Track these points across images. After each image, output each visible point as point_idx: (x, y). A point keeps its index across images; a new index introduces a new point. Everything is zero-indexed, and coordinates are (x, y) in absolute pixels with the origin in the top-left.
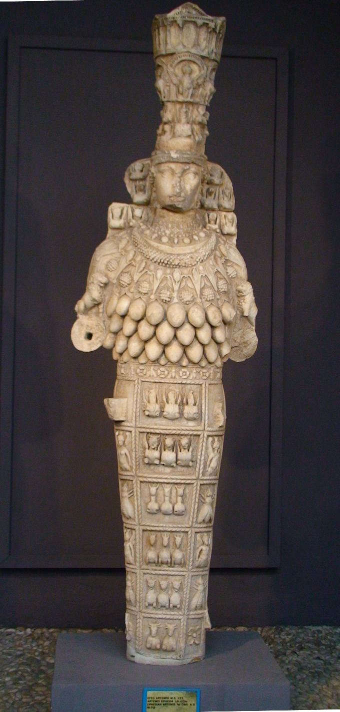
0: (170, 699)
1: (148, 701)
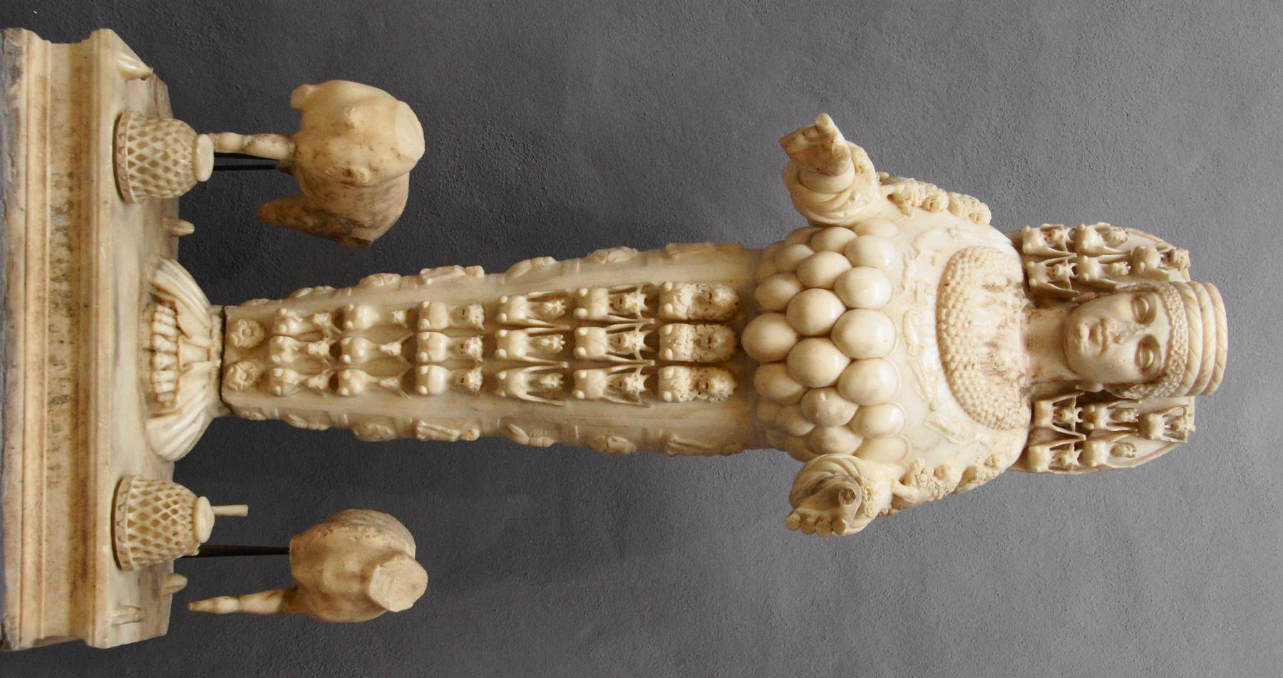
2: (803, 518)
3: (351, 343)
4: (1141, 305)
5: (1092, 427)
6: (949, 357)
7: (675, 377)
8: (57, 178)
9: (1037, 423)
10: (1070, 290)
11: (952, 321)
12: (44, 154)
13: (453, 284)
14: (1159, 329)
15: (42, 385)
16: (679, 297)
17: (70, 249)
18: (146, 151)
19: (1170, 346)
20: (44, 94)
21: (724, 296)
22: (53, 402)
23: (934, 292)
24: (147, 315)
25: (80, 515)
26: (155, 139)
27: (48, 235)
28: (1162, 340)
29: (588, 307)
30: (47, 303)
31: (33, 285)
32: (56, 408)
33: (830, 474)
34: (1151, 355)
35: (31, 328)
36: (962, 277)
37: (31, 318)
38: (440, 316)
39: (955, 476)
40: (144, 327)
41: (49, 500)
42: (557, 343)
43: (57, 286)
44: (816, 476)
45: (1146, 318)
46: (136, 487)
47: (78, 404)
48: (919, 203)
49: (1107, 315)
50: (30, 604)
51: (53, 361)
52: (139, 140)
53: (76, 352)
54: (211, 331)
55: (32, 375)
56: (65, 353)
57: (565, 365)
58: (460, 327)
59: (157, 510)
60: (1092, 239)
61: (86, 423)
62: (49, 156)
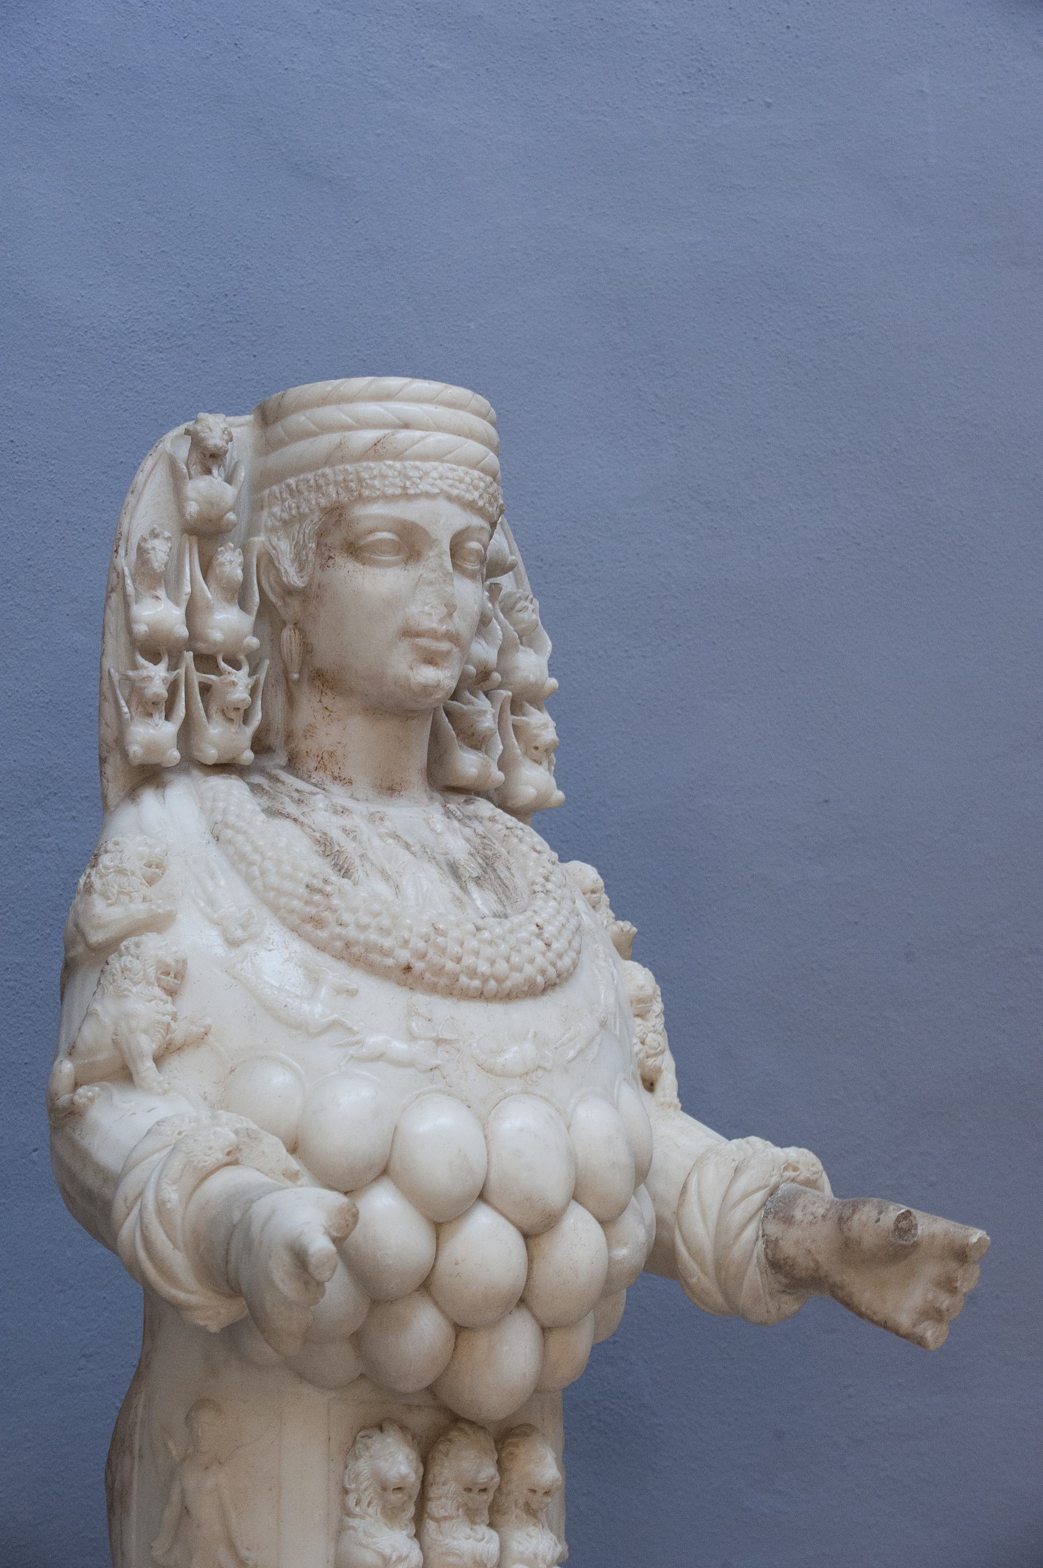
4: (377, 547)
5: (496, 676)
6: (540, 979)
10: (262, 675)
11: (484, 968)
19: (470, 506)
21: (397, 1460)
23: (421, 1000)
28: (461, 519)
33: (760, 1244)
44: (754, 1277)
45: (410, 544)
48: (170, 1007)
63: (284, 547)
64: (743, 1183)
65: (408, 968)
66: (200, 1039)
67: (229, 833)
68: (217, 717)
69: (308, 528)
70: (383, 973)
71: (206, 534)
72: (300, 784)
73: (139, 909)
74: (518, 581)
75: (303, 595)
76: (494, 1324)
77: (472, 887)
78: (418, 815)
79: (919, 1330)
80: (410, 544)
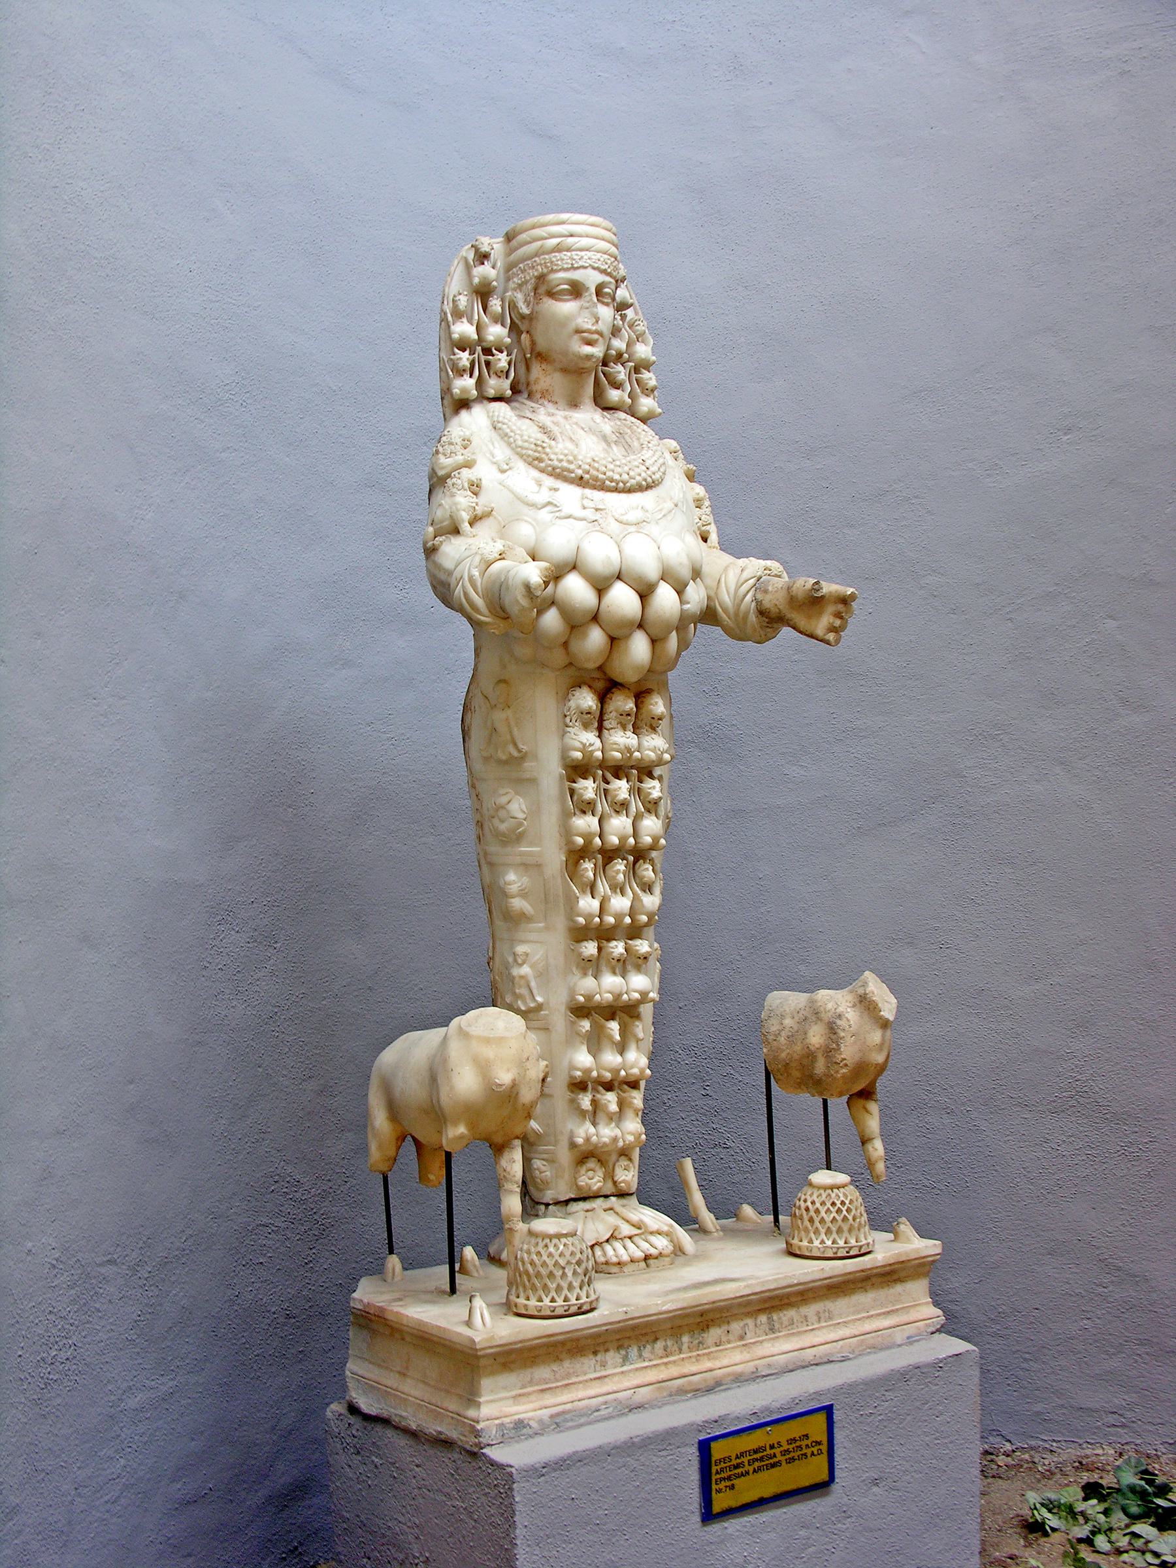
0: (769, 1452)
1: (717, 1473)
2: (833, 629)
3: (609, 1071)
4: (562, 292)
5: (626, 356)
7: (654, 750)
8: (598, 1367)
9: (626, 408)
10: (513, 356)
11: (617, 477)
12: (580, 1382)
13: (543, 974)
14: (592, 279)
15: (761, 1342)
16: (591, 745)
17: (657, 1339)
18: (576, 1284)
19: (604, 272)
20: (529, 1394)
21: (587, 700)
22: (772, 1330)
23: (588, 492)
24: (615, 1269)
25: (852, 1286)
26: (564, 1275)
27: (646, 1364)
29: (594, 835)
30: (700, 1352)
31: (694, 1368)
32: (777, 1326)
33: (754, 604)
34: (607, 290)
35: (725, 1362)
36: (570, 462)
37: (718, 1364)
38: (588, 983)
39: (699, 490)
40: (625, 1269)
41: (840, 1315)
42: (620, 866)
43: (685, 1347)
44: (753, 618)
45: (576, 290)
46: (822, 1242)
47: (773, 1304)
48: (475, 500)
49: (572, 326)
50: (913, 1315)
51: (742, 1338)
52: (565, 1292)
53: (736, 1317)
54: (587, 1211)
55: (760, 1351)
56: (736, 1326)
57: (631, 858)
58: (593, 966)
59: (845, 1219)
60: (464, 329)
61: (789, 1295)
62: (580, 1379)
63: (519, 296)
64: (745, 575)
65: (582, 478)
66: (488, 514)
67: (500, 425)
68: (493, 376)
69: (530, 287)
70: (571, 481)
71: (483, 293)
72: (533, 405)
73: (459, 458)
74: (636, 313)
75: (530, 318)
76: (628, 637)
77: (613, 445)
78: (589, 415)
79: (827, 637)
80: (576, 290)
